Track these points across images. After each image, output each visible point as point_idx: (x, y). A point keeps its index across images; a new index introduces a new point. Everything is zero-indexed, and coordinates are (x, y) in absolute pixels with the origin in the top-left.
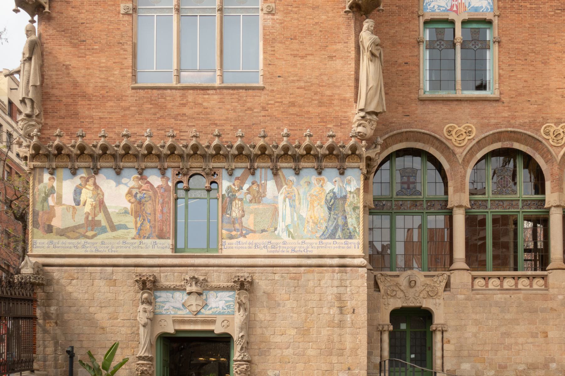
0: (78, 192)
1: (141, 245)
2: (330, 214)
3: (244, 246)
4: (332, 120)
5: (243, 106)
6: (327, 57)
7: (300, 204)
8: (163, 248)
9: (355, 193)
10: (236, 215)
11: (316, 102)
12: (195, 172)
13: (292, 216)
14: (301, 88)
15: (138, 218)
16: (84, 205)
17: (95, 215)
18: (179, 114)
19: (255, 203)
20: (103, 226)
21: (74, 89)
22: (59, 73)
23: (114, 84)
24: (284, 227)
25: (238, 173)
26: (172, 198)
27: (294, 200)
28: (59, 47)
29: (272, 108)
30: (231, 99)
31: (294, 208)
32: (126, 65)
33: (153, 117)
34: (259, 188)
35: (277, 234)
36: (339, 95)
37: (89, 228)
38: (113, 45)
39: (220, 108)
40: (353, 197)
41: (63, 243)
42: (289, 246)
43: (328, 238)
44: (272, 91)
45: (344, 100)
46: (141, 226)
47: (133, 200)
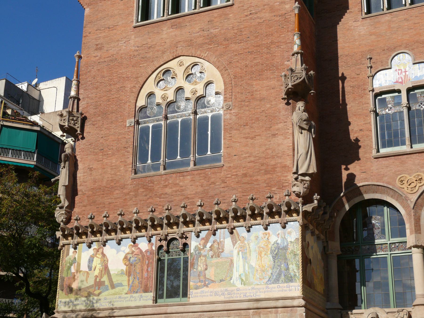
0: (91, 260)
1: (132, 299)
2: (274, 262)
3: (207, 294)
4: (276, 184)
5: (208, 182)
6: (271, 135)
7: (250, 255)
8: (146, 300)
9: (296, 243)
10: (201, 269)
11: (263, 171)
12: (172, 237)
13: (244, 266)
14: (251, 162)
15: (131, 277)
16: (94, 270)
17: (101, 277)
18: (163, 194)
19: (216, 257)
20: (106, 285)
21: (94, 184)
22: (85, 174)
23: (120, 177)
24: (238, 276)
25: (203, 234)
26: (155, 259)
27: (246, 253)
28: (87, 156)
29: (229, 180)
30: (199, 177)
31: (246, 259)
32: (128, 162)
33: (145, 198)
34: (219, 245)
35: (232, 282)
36: (281, 163)
37: (97, 288)
38: (121, 149)
39: (191, 185)
40: (293, 245)
42: (242, 292)
43: (273, 283)
44: (230, 167)
45: (285, 167)
46: (132, 283)
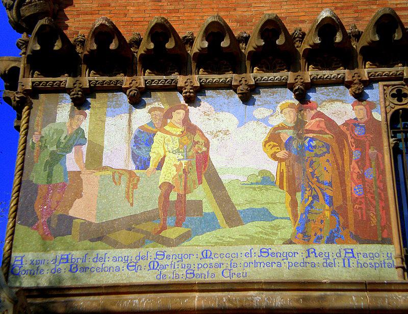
47: (282, 154)
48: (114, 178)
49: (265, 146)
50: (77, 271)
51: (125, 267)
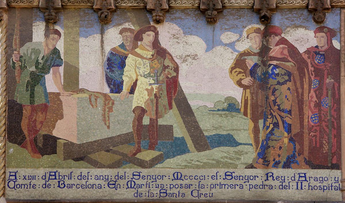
41: (81, 177)
47: (247, 81)
48: (90, 101)
49: (231, 72)
50: (64, 187)
51: (106, 186)
